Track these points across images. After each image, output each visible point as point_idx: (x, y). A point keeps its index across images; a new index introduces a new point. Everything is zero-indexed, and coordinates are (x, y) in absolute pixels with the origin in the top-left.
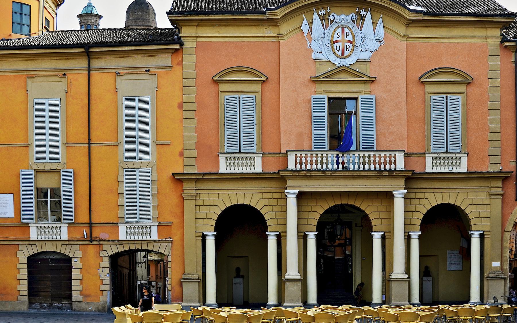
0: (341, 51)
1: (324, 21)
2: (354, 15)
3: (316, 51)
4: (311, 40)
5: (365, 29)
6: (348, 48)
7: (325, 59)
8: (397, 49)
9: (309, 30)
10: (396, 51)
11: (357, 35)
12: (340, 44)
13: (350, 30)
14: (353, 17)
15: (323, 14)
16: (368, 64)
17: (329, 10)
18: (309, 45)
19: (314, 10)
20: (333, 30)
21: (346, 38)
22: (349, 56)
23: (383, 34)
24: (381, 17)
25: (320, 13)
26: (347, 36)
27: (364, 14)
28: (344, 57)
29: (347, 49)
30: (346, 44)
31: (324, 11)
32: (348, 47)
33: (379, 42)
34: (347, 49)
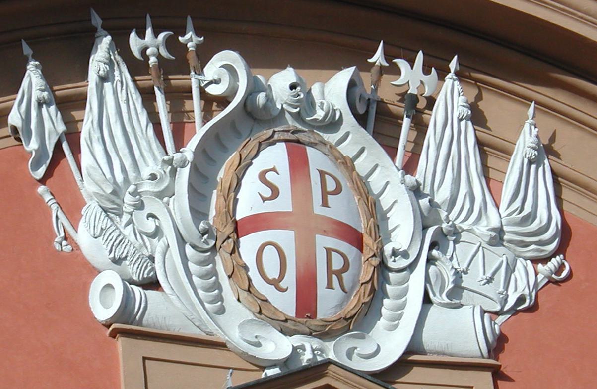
0: (290, 280)
6: (339, 274)
12: (285, 238)
17: (190, 39)
21: (325, 204)
26: (325, 193)
29: (335, 277)
30: (323, 242)
31: (162, 36)
32: (337, 263)
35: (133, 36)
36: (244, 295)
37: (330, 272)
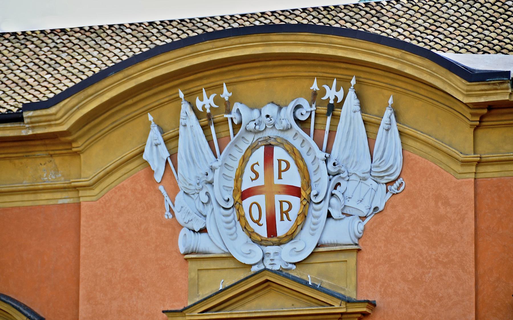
0: (264, 221)
1: (212, 128)
2: (304, 102)
3: (190, 225)
4: (174, 190)
5: (343, 145)
7: (215, 250)
8: (446, 203)
9: (167, 161)
10: (442, 210)
11: (315, 167)
12: (260, 199)
13: (293, 152)
14: (298, 112)
15: (207, 107)
16: (352, 259)
17: (226, 94)
18: (171, 211)
19: (181, 95)
20: (239, 156)
21: (280, 178)
22: (291, 237)
23: (400, 159)
24: (391, 101)
25: (199, 105)
26: (280, 171)
27: (336, 99)
28: (275, 239)
29: (284, 215)
30: (278, 198)
31: (212, 96)
32: (286, 207)
33: (386, 184)
34: (284, 215)
35: (197, 100)
36: (244, 230)
37: (282, 212)
